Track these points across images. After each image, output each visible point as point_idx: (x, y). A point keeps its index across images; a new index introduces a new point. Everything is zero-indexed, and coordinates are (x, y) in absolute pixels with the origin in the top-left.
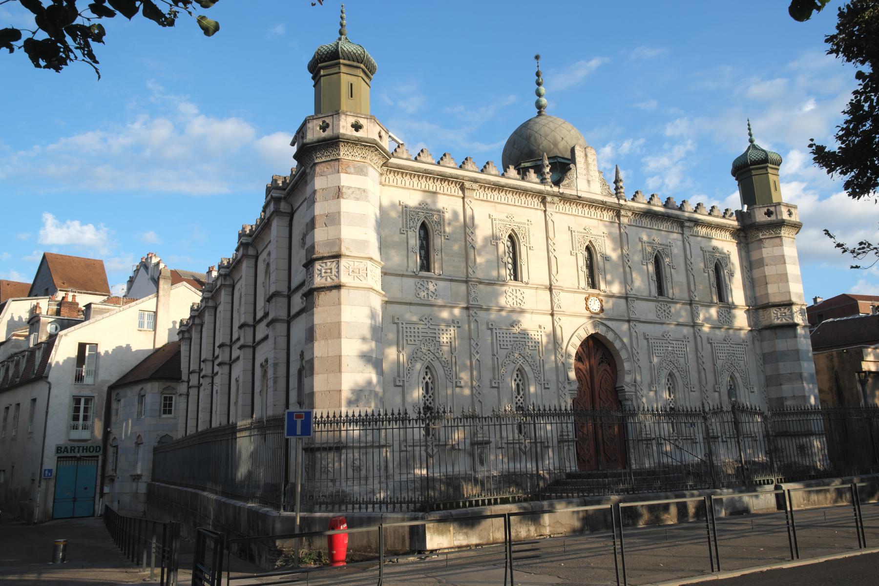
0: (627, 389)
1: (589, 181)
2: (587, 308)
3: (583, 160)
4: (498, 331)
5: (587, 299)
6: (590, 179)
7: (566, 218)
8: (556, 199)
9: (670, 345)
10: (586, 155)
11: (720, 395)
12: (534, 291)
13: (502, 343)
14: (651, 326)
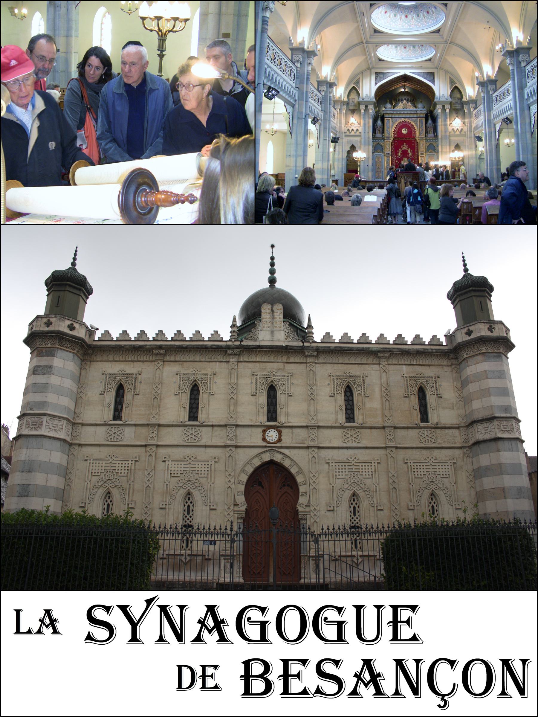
0: (300, 509)
1: (272, 332)
2: (264, 439)
3: (268, 316)
4: (170, 463)
5: (264, 432)
6: (274, 329)
7: (250, 365)
8: (237, 351)
9: (354, 467)
10: (273, 311)
11: (414, 513)
12: (210, 429)
13: (173, 472)
14: (335, 451)
